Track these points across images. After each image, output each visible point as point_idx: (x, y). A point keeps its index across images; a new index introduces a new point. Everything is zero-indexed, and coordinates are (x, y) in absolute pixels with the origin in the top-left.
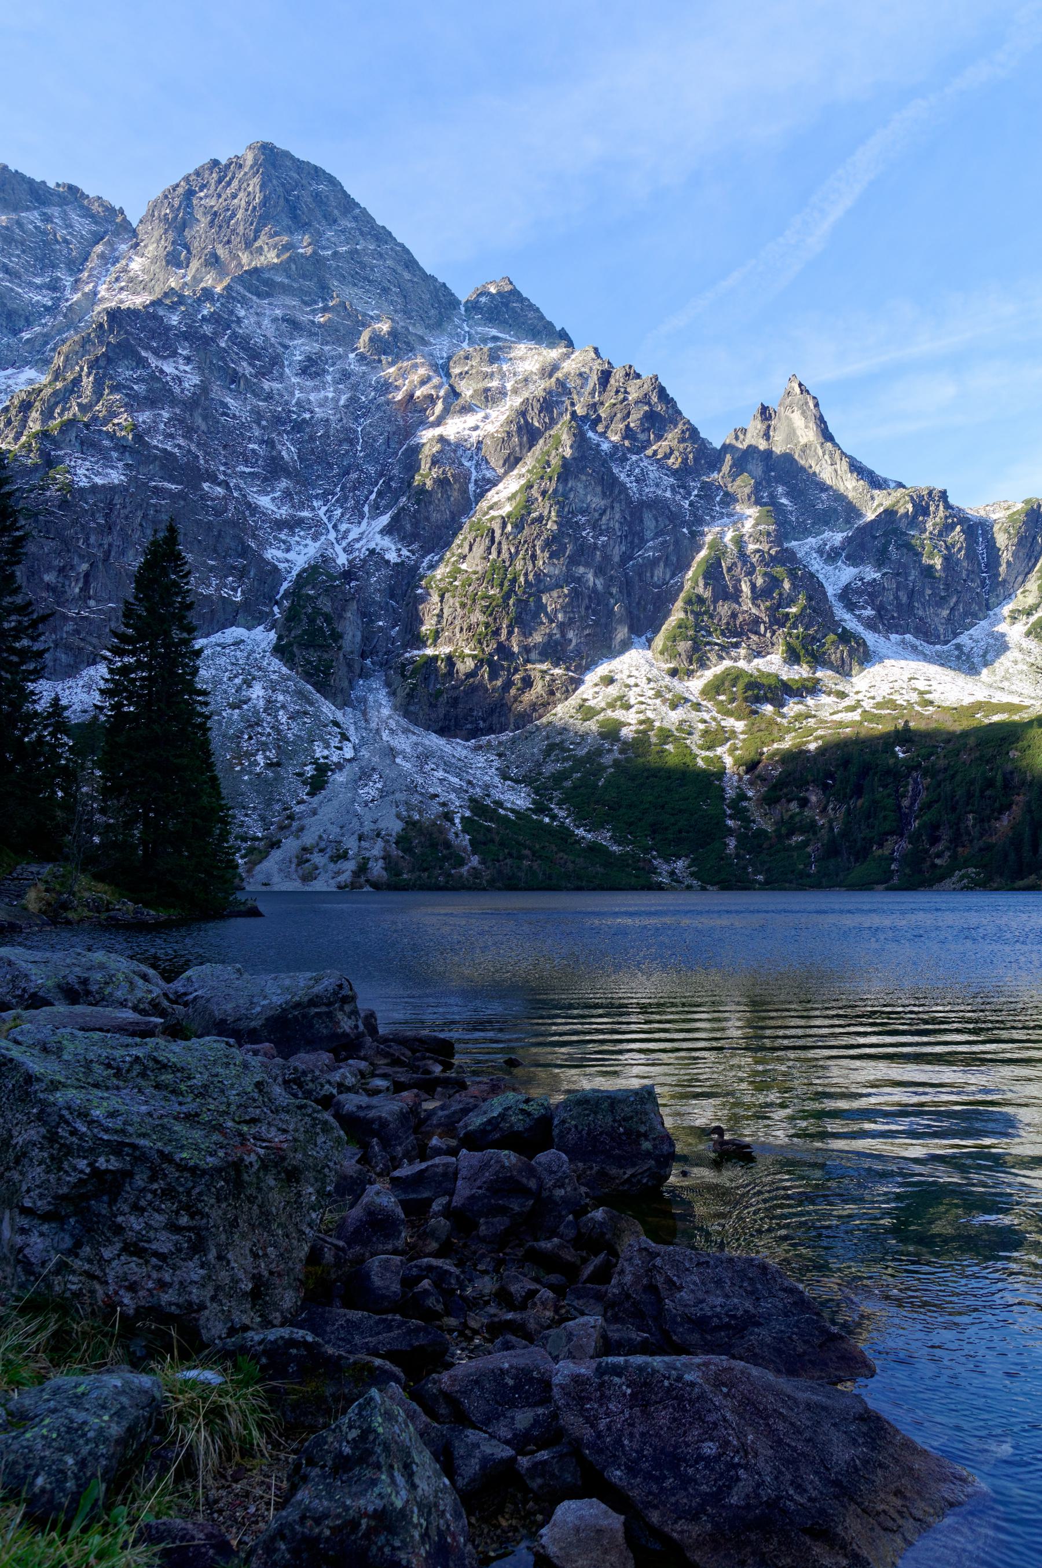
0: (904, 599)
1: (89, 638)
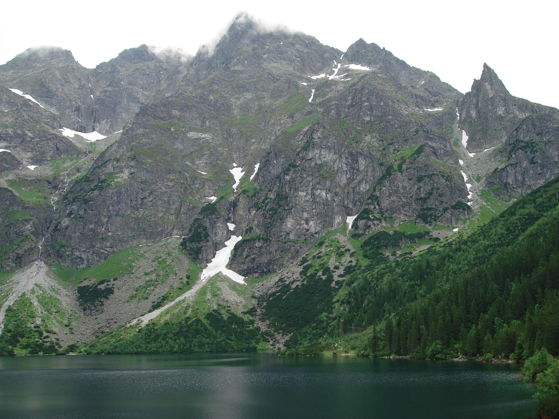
0: (520, 178)
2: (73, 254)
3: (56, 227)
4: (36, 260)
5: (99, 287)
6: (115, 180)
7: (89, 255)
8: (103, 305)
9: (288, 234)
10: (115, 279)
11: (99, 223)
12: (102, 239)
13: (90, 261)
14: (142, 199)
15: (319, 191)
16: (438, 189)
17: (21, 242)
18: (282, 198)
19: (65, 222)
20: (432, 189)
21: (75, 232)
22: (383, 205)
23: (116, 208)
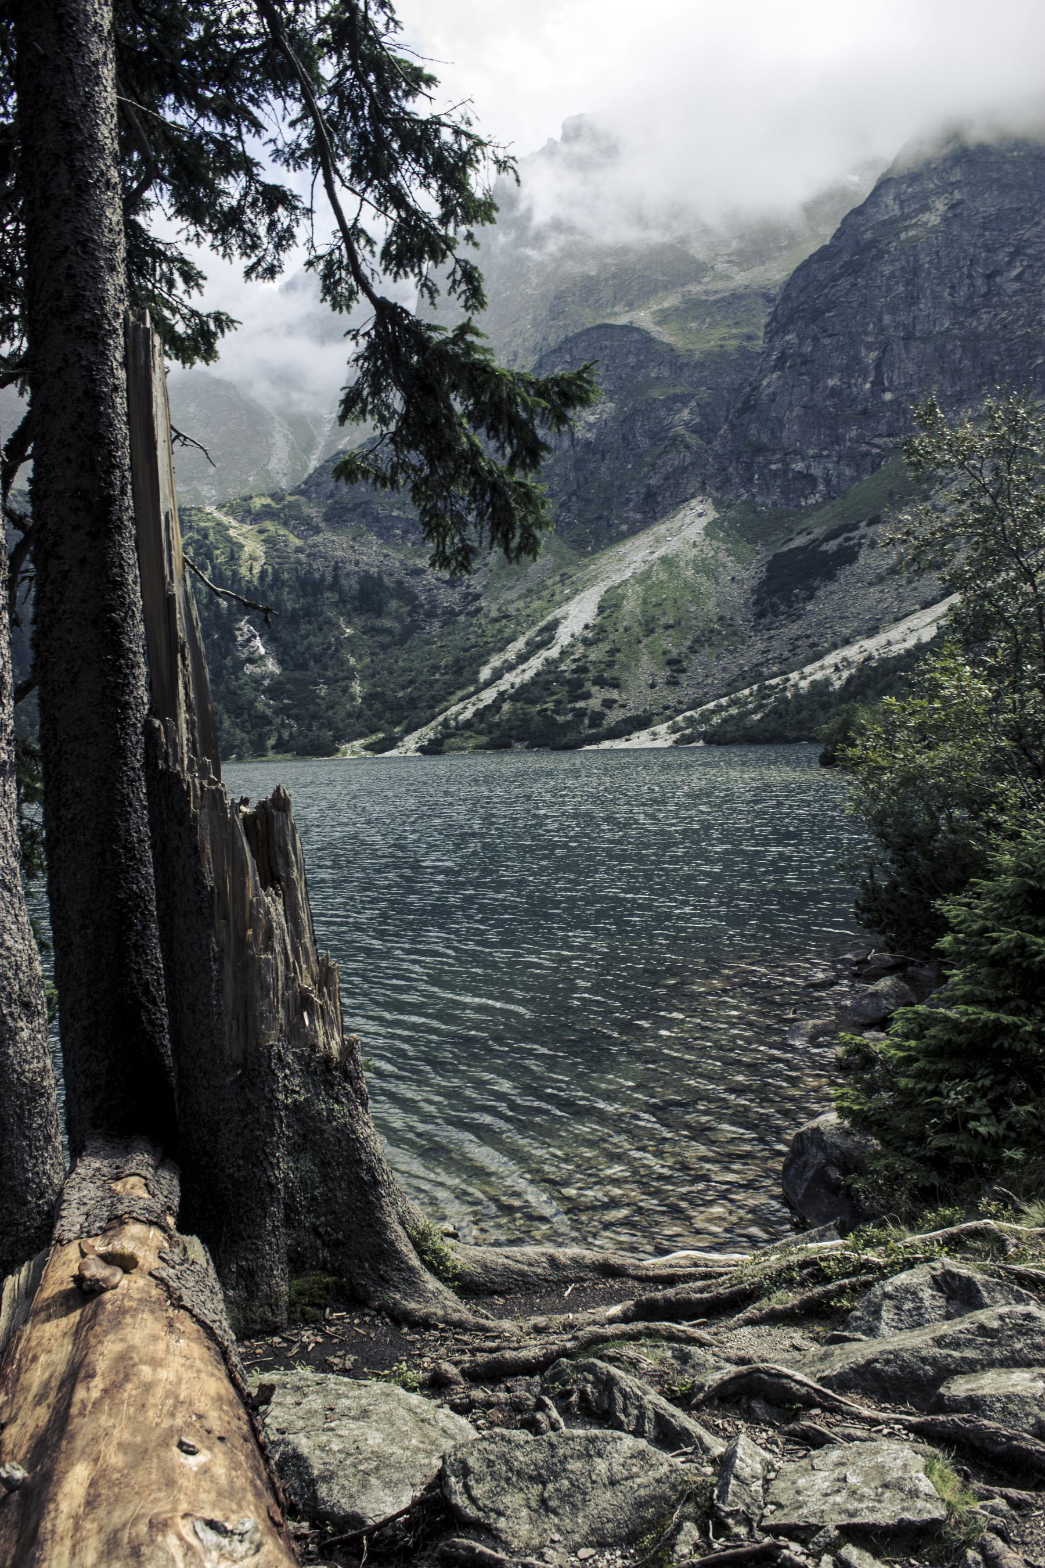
1: (876, 441)
2: (786, 464)
3: (746, 402)
4: (693, 496)
5: (825, 547)
6: (903, 236)
7: (830, 466)
8: (810, 598)
10: (874, 521)
11: (853, 367)
12: (865, 412)
13: (834, 481)
14: (990, 277)
17: (659, 456)
19: (770, 381)
21: (791, 407)
23: (903, 317)
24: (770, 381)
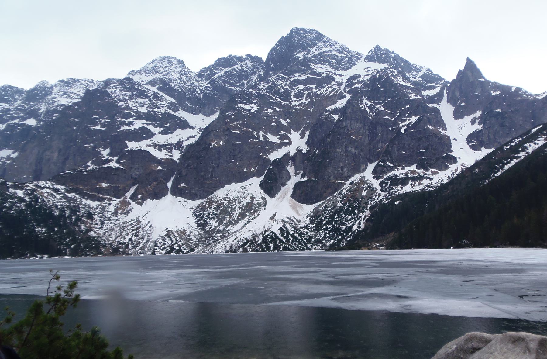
0: (492, 137)
9: (329, 177)
15: (350, 149)
16: (432, 146)
18: (324, 154)
20: (428, 145)
22: (393, 157)
23: (217, 162)
24: (184, 172)
